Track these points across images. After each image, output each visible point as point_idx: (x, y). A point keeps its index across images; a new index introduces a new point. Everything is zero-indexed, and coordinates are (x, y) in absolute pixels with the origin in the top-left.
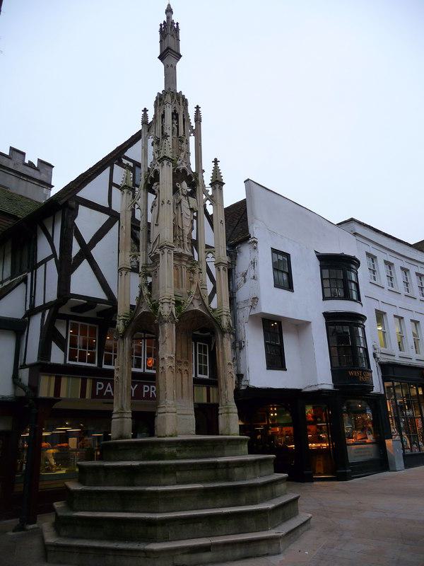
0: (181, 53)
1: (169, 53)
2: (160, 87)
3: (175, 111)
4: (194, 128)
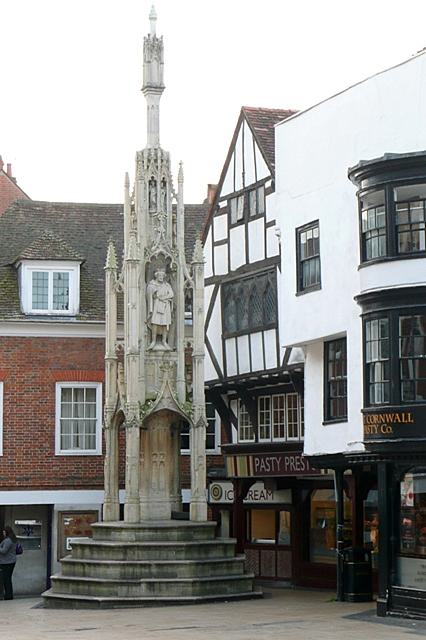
0: (166, 83)
1: (154, 88)
2: (142, 143)
3: (153, 177)
4: (176, 192)
